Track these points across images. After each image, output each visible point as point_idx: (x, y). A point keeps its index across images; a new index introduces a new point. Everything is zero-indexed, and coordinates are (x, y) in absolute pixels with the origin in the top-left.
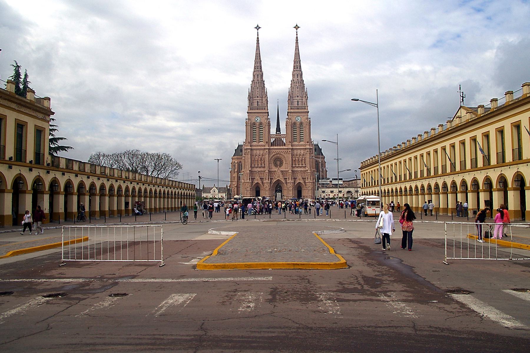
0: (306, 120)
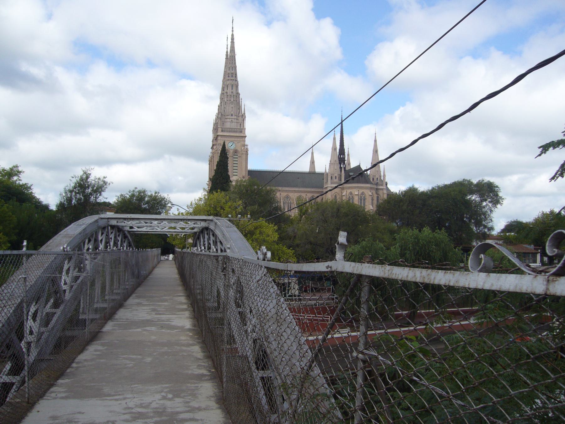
0: (243, 148)
